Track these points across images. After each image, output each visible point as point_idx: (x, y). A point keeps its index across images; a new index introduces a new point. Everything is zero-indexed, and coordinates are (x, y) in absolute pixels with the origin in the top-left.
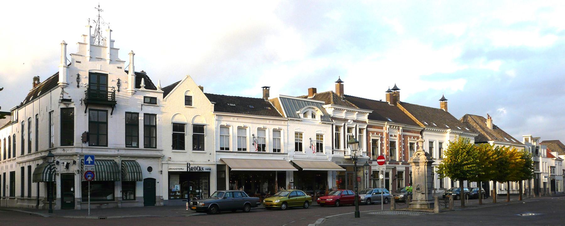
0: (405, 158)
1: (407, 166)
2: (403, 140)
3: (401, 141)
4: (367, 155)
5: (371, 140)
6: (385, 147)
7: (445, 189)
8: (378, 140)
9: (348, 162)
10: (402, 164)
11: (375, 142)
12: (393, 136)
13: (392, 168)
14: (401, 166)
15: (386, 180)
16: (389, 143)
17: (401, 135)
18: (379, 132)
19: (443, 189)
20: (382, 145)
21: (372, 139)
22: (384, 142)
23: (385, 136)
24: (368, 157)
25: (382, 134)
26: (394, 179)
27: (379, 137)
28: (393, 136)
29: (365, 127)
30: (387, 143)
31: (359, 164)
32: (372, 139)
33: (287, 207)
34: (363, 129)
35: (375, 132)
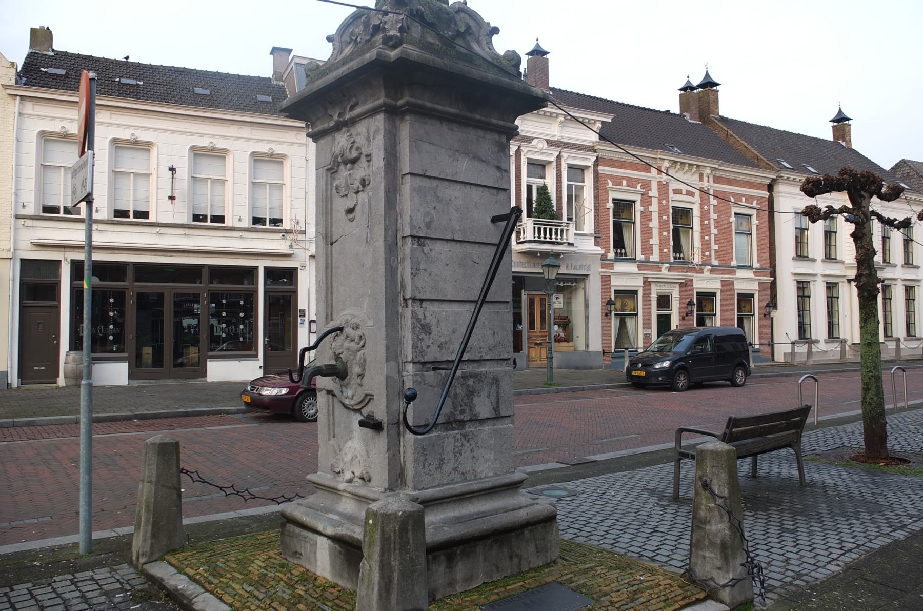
0: (725, 253)
1: (727, 277)
2: (714, 206)
3: (709, 210)
4: (597, 244)
5: (611, 200)
6: (654, 224)
7: (843, 342)
8: (634, 202)
9: (529, 262)
10: (711, 272)
11: (623, 207)
12: (684, 192)
13: (681, 284)
14: (705, 278)
15: (658, 316)
16: (671, 211)
17: (708, 189)
18: (639, 181)
19: (837, 342)
20: (647, 216)
21: (613, 199)
22: (654, 207)
23: (654, 192)
24: (599, 248)
25: (647, 185)
26: (687, 314)
27: (636, 193)
28: (684, 192)
29: (590, 163)
30: (662, 211)
31: (568, 267)
32: (613, 199)
33: (689, 381)
34: (582, 169)
35: (623, 178)
